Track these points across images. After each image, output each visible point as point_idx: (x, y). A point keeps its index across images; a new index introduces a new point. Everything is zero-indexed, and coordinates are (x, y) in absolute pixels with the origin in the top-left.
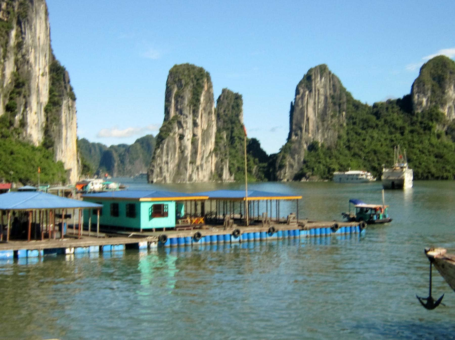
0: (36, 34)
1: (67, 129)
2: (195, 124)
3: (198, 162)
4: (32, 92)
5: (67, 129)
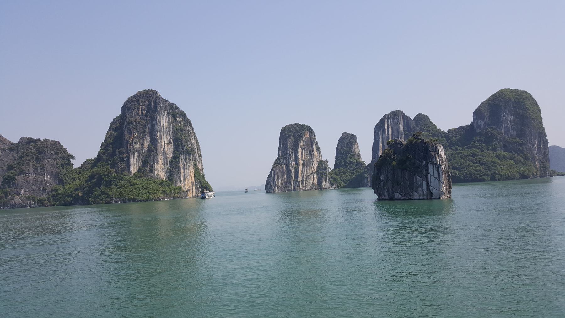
0: (160, 124)
1: (184, 170)
2: (297, 158)
3: (300, 179)
4: (158, 153)
5: (184, 170)
